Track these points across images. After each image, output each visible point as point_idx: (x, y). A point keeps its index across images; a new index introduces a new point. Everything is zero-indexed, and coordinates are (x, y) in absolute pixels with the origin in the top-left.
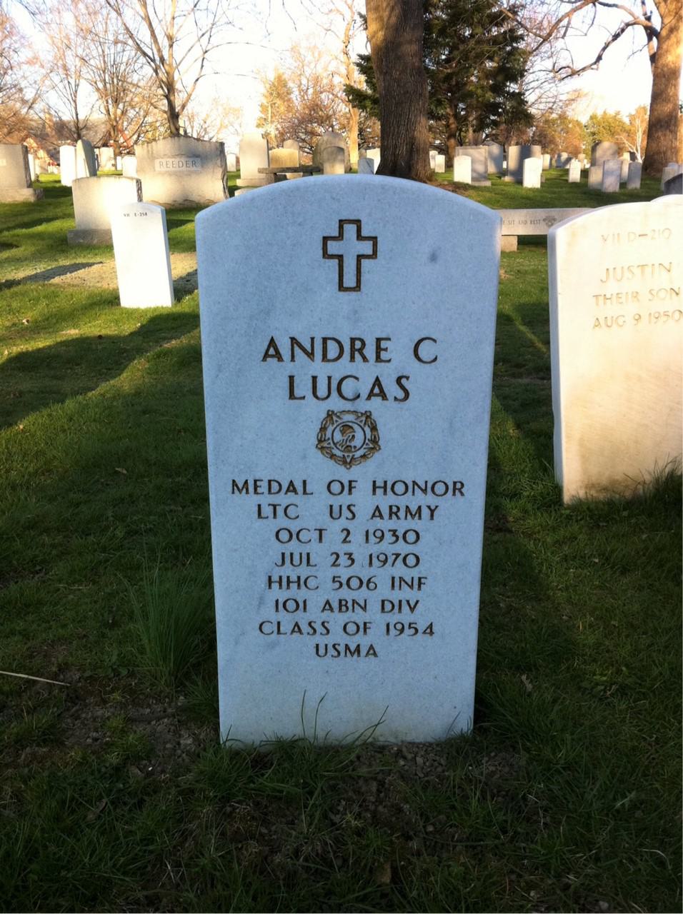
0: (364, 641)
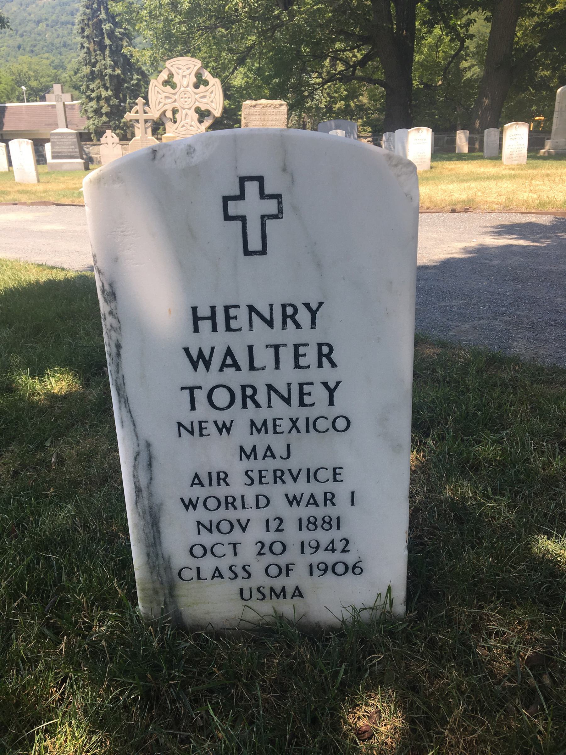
0: (290, 583)
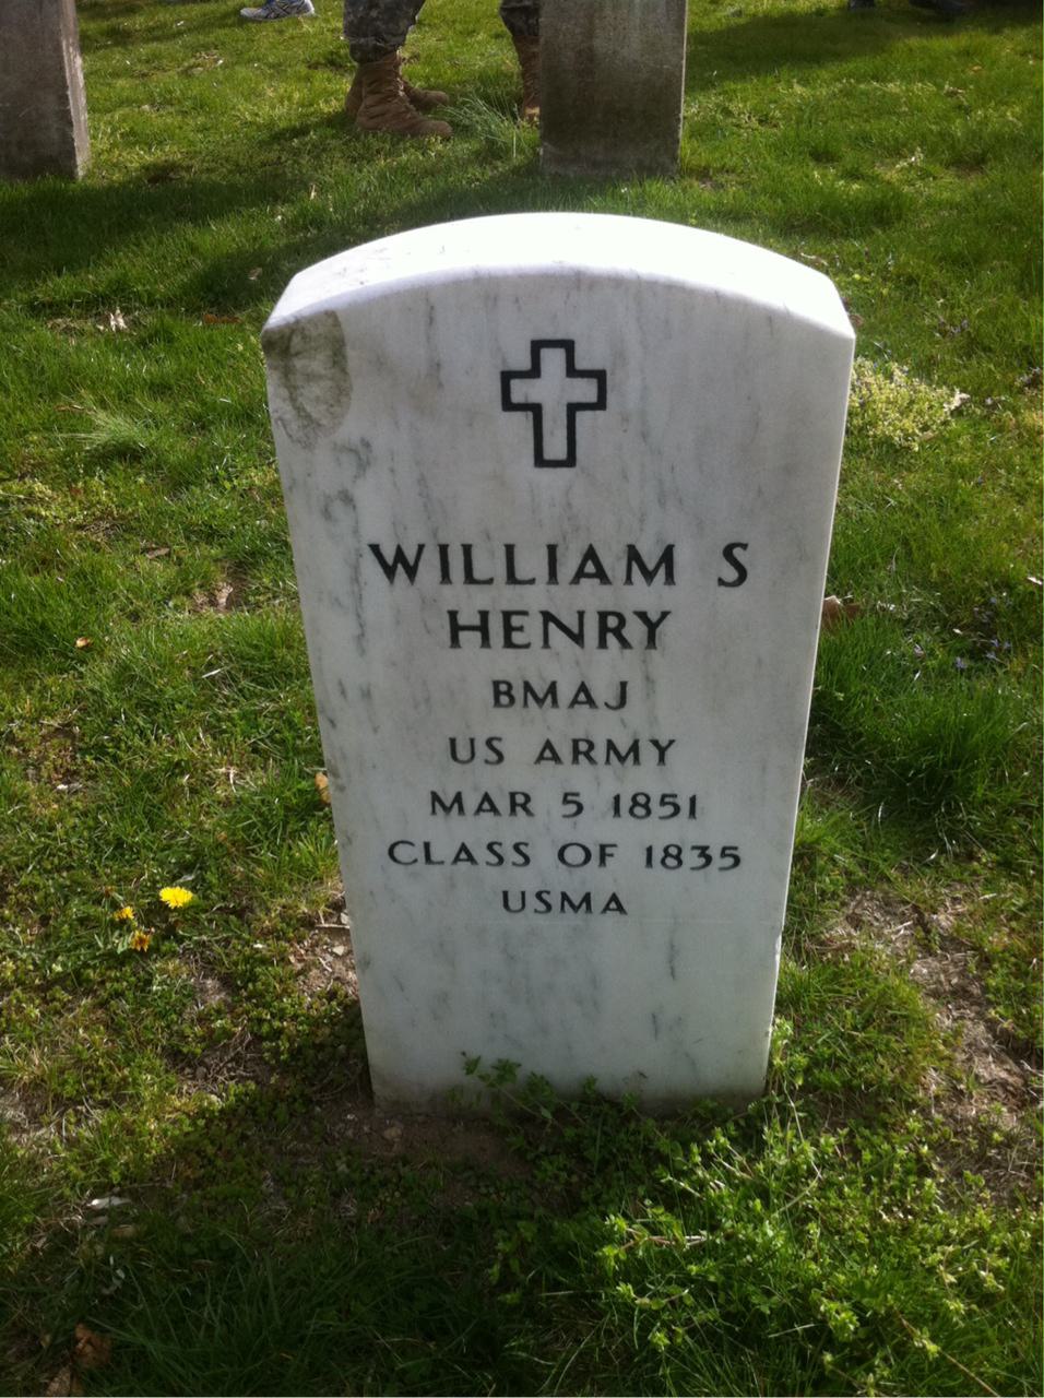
0: (598, 880)
